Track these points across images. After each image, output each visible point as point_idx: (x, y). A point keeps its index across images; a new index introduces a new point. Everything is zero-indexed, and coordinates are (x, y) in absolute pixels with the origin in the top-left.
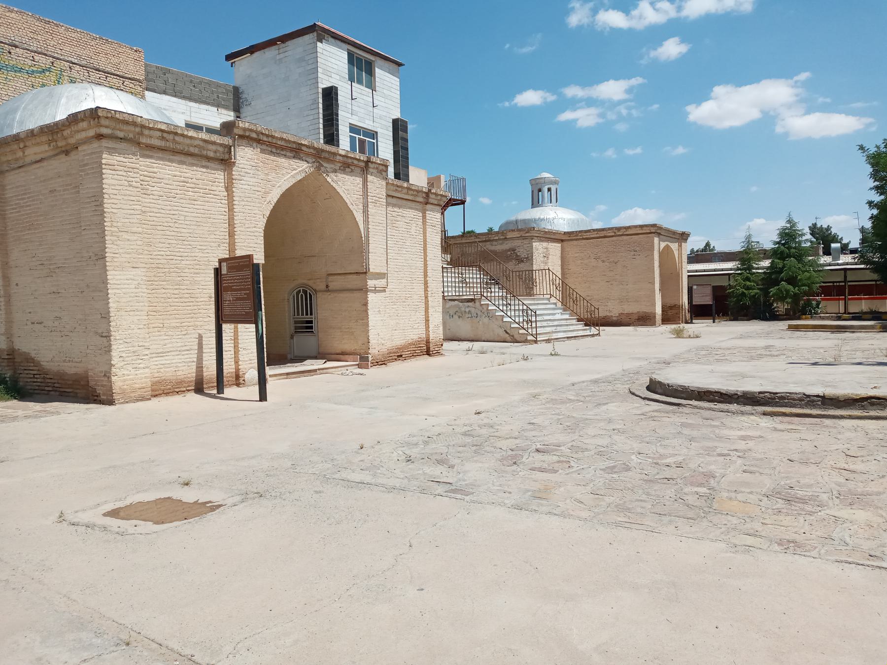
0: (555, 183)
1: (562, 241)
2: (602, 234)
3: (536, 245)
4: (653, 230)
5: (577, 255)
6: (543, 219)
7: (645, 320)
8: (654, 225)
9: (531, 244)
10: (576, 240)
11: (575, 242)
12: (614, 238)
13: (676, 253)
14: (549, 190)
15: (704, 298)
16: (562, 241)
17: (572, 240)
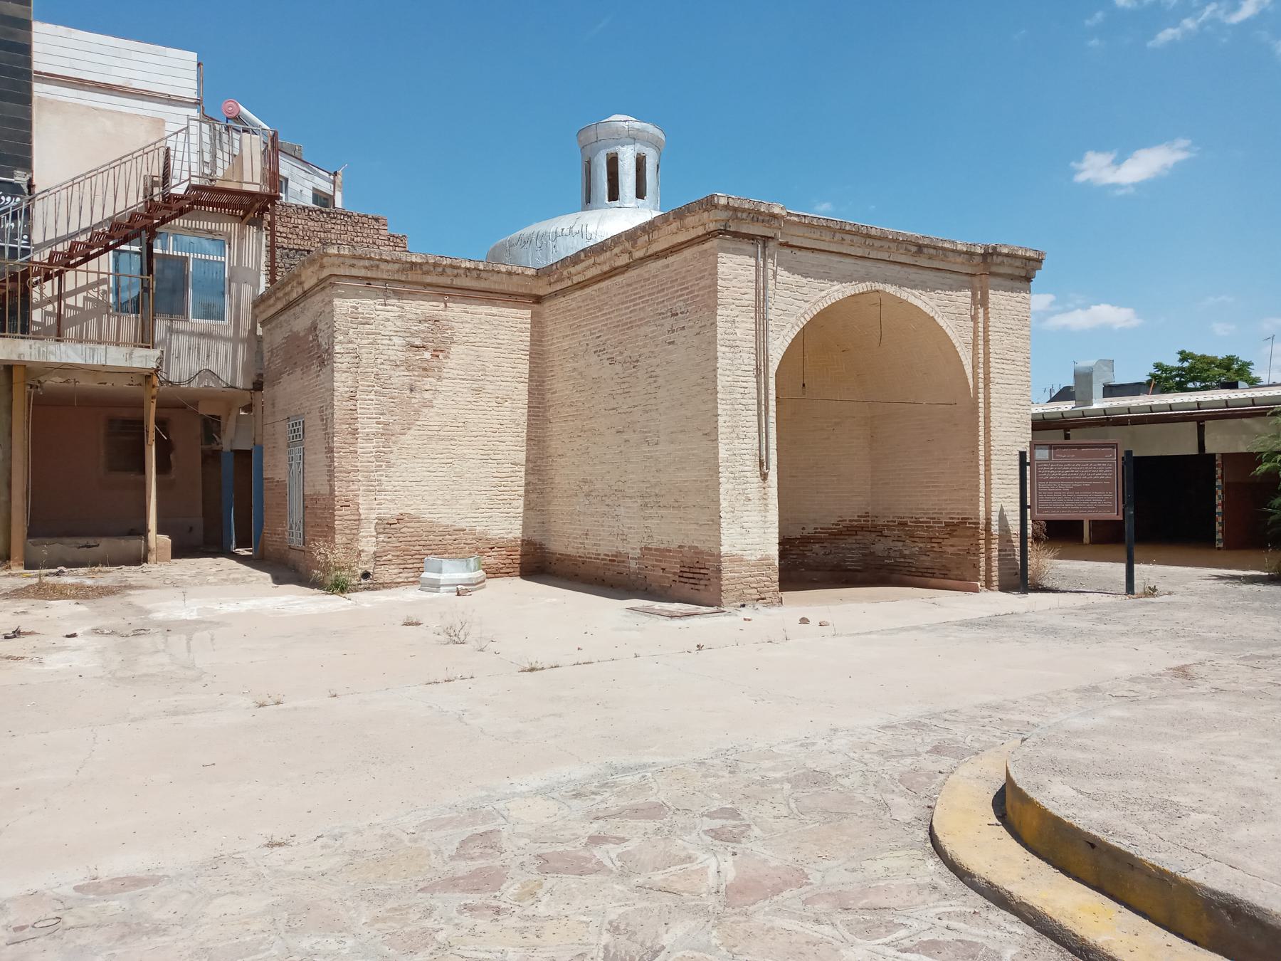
0: (633, 138)
1: (538, 300)
2: (606, 261)
3: (343, 306)
4: (711, 221)
5: (565, 344)
6: (526, 241)
7: (688, 580)
8: (708, 204)
9: (331, 302)
10: (563, 292)
11: (561, 302)
12: (632, 274)
13: (957, 331)
14: (613, 162)
15: (1098, 495)
16: (538, 300)
17: (556, 294)
